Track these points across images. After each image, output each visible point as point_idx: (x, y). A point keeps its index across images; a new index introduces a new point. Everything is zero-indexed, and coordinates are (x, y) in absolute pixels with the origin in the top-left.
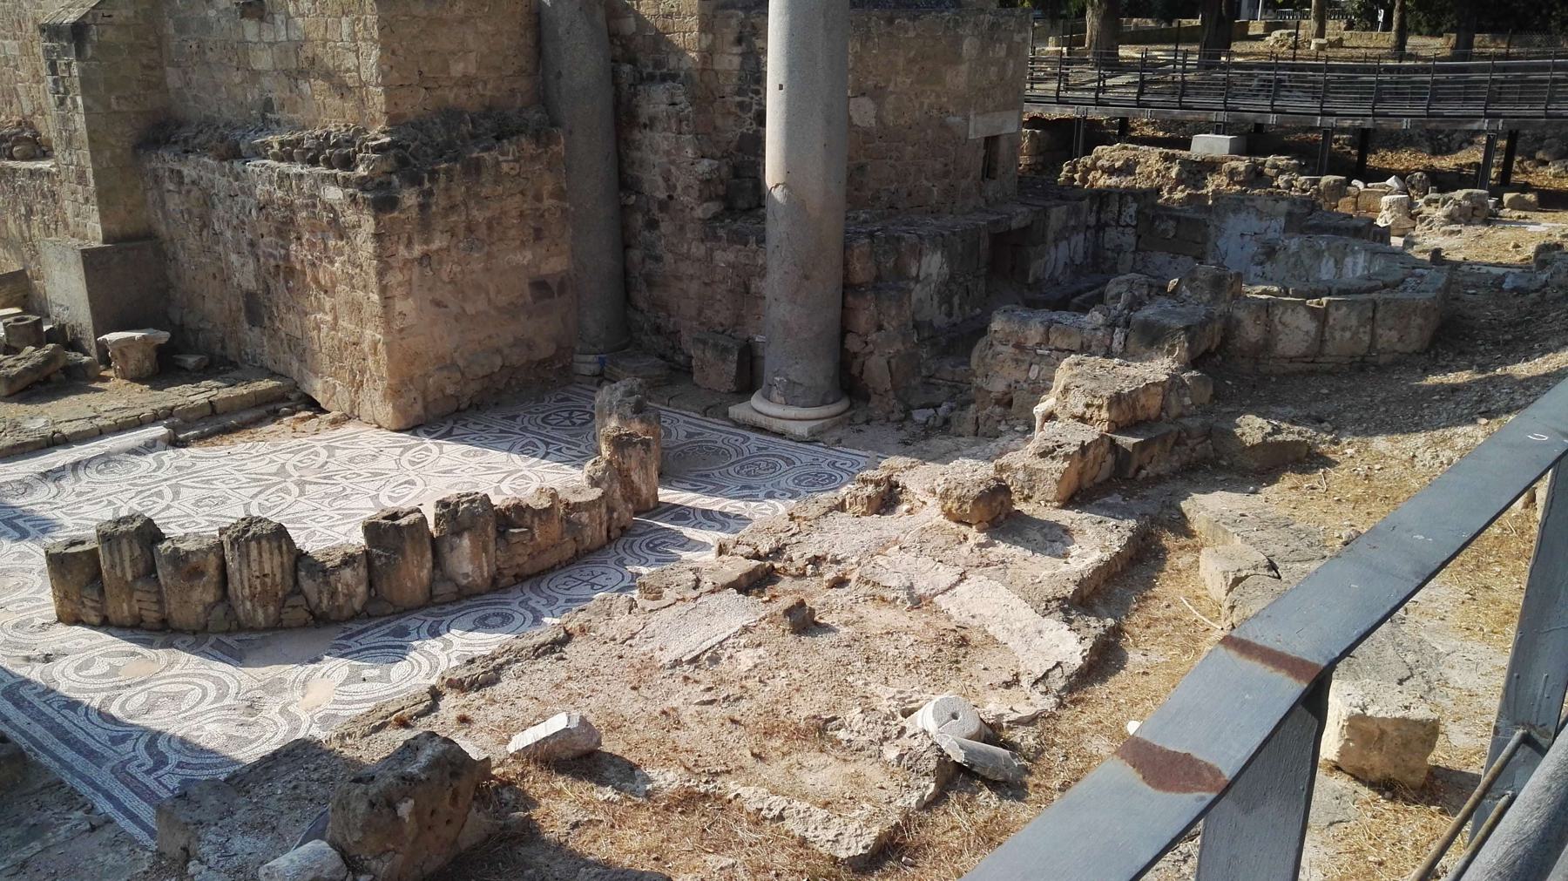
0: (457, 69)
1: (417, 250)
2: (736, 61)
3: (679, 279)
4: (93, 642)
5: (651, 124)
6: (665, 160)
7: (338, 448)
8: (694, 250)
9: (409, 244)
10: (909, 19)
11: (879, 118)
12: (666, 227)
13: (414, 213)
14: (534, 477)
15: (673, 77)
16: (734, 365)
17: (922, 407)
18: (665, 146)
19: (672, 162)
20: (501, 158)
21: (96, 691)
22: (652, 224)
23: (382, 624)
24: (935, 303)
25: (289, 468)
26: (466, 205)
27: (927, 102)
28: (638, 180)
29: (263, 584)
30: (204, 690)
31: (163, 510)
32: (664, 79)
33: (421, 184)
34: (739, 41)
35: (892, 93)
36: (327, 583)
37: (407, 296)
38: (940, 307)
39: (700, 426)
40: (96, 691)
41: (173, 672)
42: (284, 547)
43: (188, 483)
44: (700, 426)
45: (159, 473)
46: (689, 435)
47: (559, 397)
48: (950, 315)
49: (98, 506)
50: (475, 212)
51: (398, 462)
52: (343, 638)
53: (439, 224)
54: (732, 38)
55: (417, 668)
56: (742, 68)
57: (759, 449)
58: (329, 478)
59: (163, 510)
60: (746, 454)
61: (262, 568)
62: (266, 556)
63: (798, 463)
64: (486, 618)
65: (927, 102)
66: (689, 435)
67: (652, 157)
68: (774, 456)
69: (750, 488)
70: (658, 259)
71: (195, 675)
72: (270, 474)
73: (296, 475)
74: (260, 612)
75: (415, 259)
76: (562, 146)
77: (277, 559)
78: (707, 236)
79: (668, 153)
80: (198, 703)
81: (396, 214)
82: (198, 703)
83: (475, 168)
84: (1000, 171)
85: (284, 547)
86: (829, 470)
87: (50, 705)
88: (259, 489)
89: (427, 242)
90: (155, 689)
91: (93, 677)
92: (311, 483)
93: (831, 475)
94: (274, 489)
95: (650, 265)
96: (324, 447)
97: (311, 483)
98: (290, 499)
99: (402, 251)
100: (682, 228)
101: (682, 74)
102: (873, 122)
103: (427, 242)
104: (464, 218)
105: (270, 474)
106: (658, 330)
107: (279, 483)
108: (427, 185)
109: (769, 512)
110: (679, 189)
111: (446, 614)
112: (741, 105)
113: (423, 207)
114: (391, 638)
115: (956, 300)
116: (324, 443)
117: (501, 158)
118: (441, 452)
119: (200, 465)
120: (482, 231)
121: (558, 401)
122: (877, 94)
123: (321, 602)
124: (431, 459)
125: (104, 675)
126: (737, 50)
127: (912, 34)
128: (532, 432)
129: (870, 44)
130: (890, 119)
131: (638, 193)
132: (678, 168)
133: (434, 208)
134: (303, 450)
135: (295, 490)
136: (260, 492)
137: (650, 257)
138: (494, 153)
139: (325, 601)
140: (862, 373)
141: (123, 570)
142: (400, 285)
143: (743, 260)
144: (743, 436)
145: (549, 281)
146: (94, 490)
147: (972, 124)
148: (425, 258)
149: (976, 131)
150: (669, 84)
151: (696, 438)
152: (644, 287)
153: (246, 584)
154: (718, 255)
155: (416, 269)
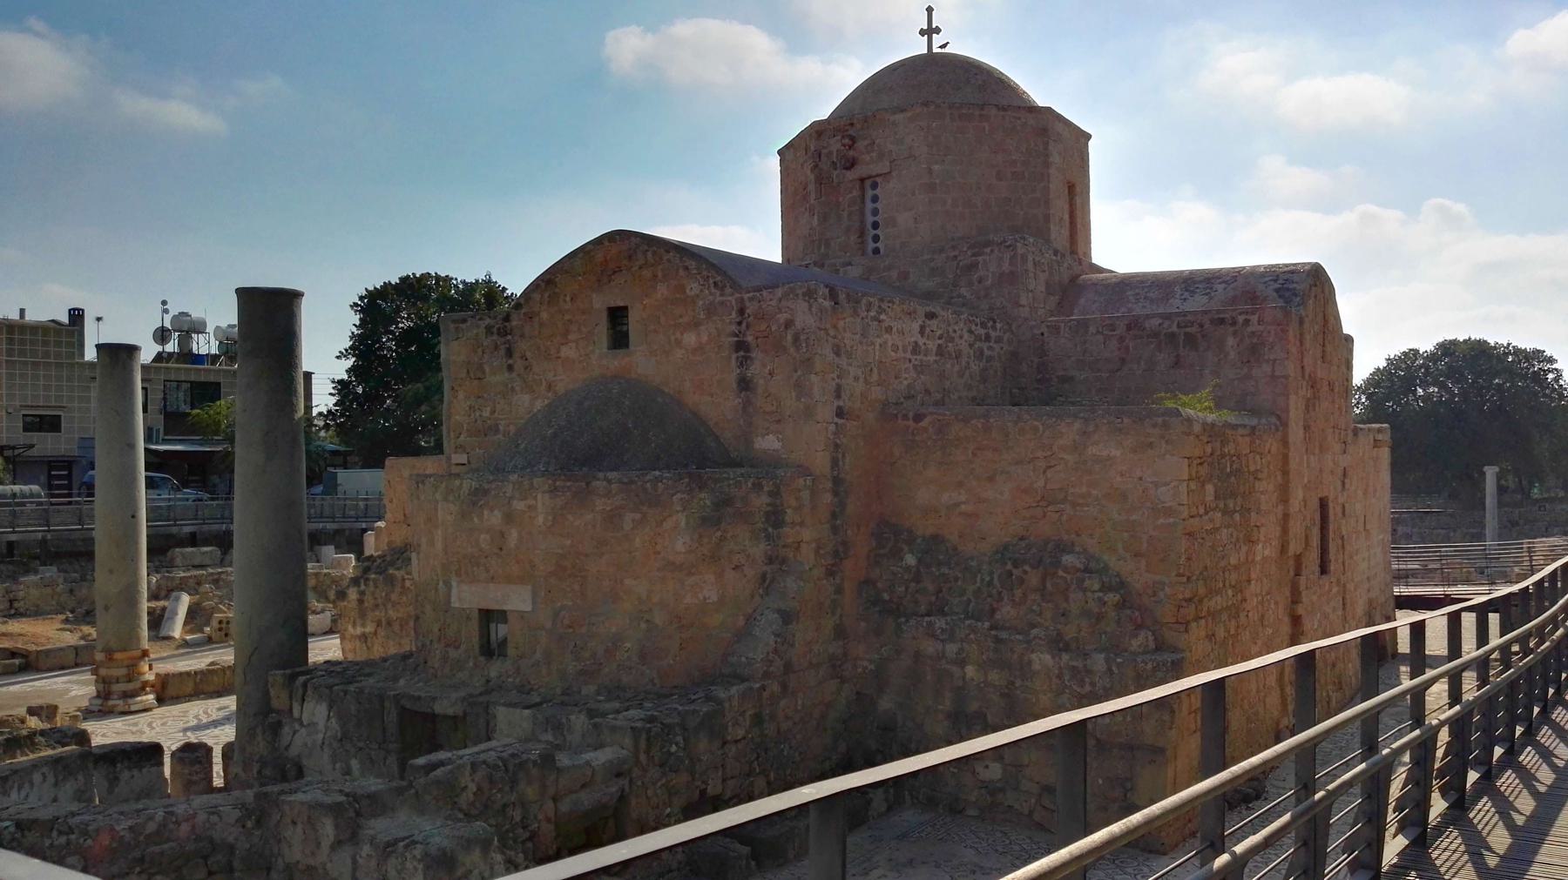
1: (359, 630)
13: (354, 604)
20: (406, 577)
26: (384, 605)
33: (359, 586)
50: (391, 612)
75: (357, 636)
81: (345, 603)
83: (391, 581)
89: (363, 625)
103: (363, 625)
104: (383, 614)
108: (363, 587)
113: (361, 601)
117: (406, 577)
120: (396, 627)
138: (402, 572)
147: (454, 591)
155: (358, 643)
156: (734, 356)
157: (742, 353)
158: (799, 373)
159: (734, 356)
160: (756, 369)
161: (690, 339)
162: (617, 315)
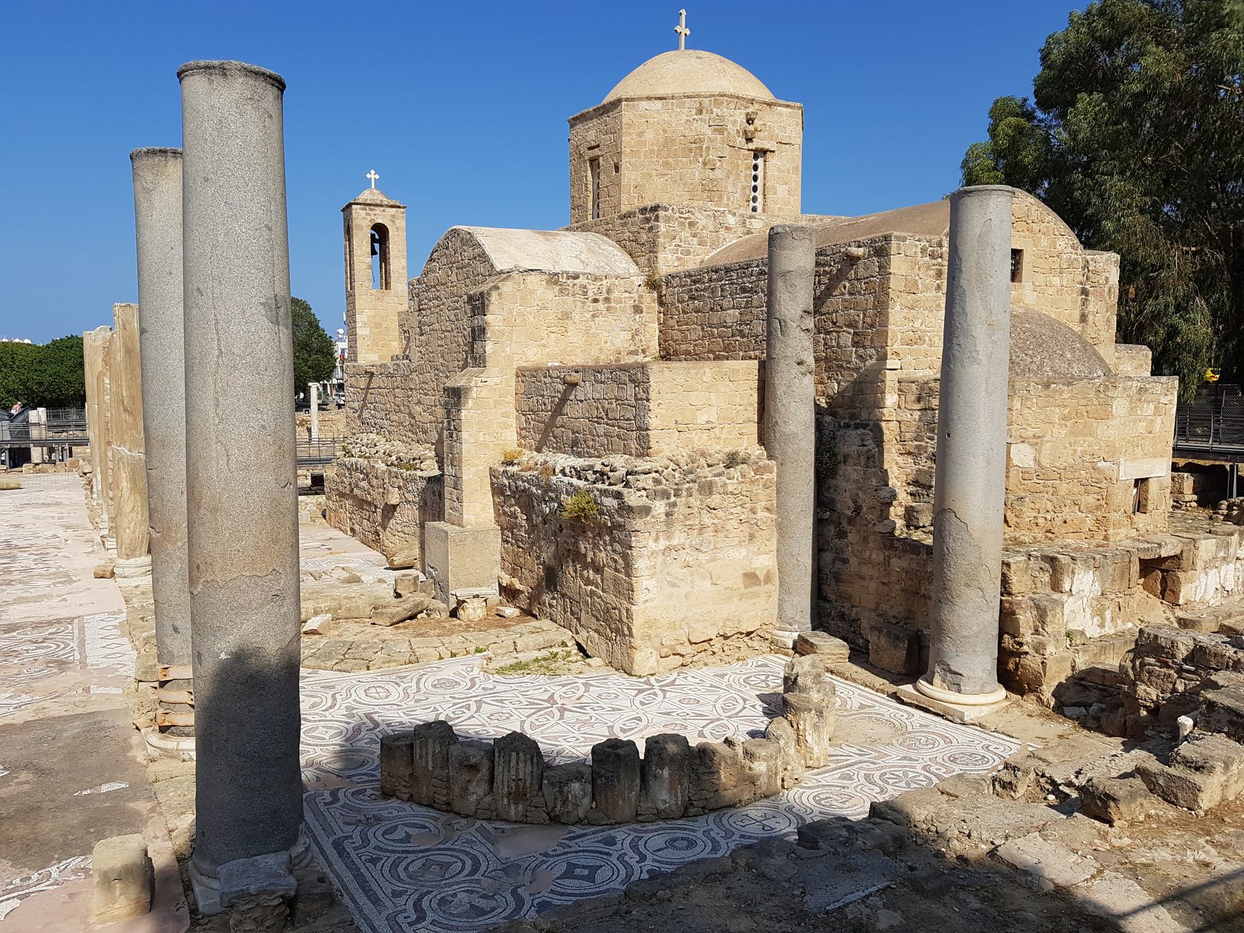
0: (702, 418)
1: (662, 543)
2: (917, 415)
3: (862, 578)
4: (401, 813)
5: (846, 459)
6: (855, 486)
7: (592, 685)
8: (874, 556)
9: (657, 540)
10: (1064, 384)
11: (1037, 461)
12: (852, 537)
13: (663, 517)
14: (730, 726)
15: (865, 426)
16: (905, 652)
17: (1074, 705)
18: (855, 476)
19: (860, 489)
21: (392, 851)
22: (842, 534)
23: (598, 831)
24: (1088, 616)
25: (556, 697)
27: (1079, 449)
28: (833, 501)
29: (517, 786)
30: (464, 863)
31: (469, 718)
32: (857, 427)
33: (668, 498)
34: (919, 400)
35: (1048, 441)
36: (561, 792)
37: (652, 576)
38: (1093, 618)
39: (872, 700)
40: (392, 851)
41: (446, 846)
42: (535, 760)
43: (488, 700)
44: (872, 700)
45: (470, 691)
46: (862, 706)
47: (760, 663)
48: (1102, 626)
49: (427, 711)
51: (632, 702)
52: (567, 839)
53: (678, 526)
54: (913, 398)
55: (616, 874)
56: (920, 420)
57: (921, 726)
58: (582, 708)
59: (469, 718)
60: (910, 729)
61: (517, 774)
62: (521, 765)
63: (955, 742)
64: (675, 840)
65: (1079, 449)
66: (862, 706)
67: (844, 484)
68: (934, 733)
69: (910, 759)
70: (846, 561)
71: (460, 851)
72: (542, 700)
73: (560, 702)
74: (513, 807)
76: (775, 474)
77: (529, 768)
78: (885, 546)
79: (857, 482)
80: (457, 874)
82: (457, 874)
84: (1150, 507)
85: (535, 760)
86: (982, 752)
87: (360, 858)
88: (534, 711)
89: (669, 538)
90: (431, 857)
91: (393, 840)
92: (569, 710)
93: (984, 757)
94: (542, 712)
95: (838, 565)
96: (583, 684)
97: (569, 710)
98: (553, 721)
99: (652, 545)
100: (865, 539)
101: (871, 423)
102: (1032, 463)
103: (669, 538)
105: (542, 700)
106: (842, 617)
107: (548, 708)
108: (673, 499)
109: (924, 783)
110: (865, 509)
111: (646, 832)
112: (918, 447)
114: (602, 845)
115: (1108, 614)
116: (584, 681)
117: (728, 481)
118: (665, 697)
119: (500, 688)
121: (759, 666)
122: (1036, 441)
123: (555, 807)
124: (656, 702)
125: (401, 841)
126: (918, 406)
127: (1065, 396)
128: (735, 689)
129: (1029, 403)
130: (1045, 462)
131: (833, 510)
132: (864, 493)
133: (676, 515)
134: (567, 685)
135: (557, 714)
136: (534, 713)
137: (840, 560)
138: (723, 478)
139: (559, 807)
140: (1017, 669)
141: (427, 762)
142: (647, 568)
143: (914, 566)
144: (908, 713)
145: (758, 573)
146: (427, 699)
148: (669, 548)
149: (1125, 474)
150: (860, 431)
151: (867, 710)
152: (833, 582)
153: (506, 783)
154: (894, 561)
155: (661, 557)
156: (1080, 298)
157: (1083, 297)
158: (1109, 313)
159: (1080, 298)
160: (1091, 307)
161: (1056, 281)
162: (1016, 254)
